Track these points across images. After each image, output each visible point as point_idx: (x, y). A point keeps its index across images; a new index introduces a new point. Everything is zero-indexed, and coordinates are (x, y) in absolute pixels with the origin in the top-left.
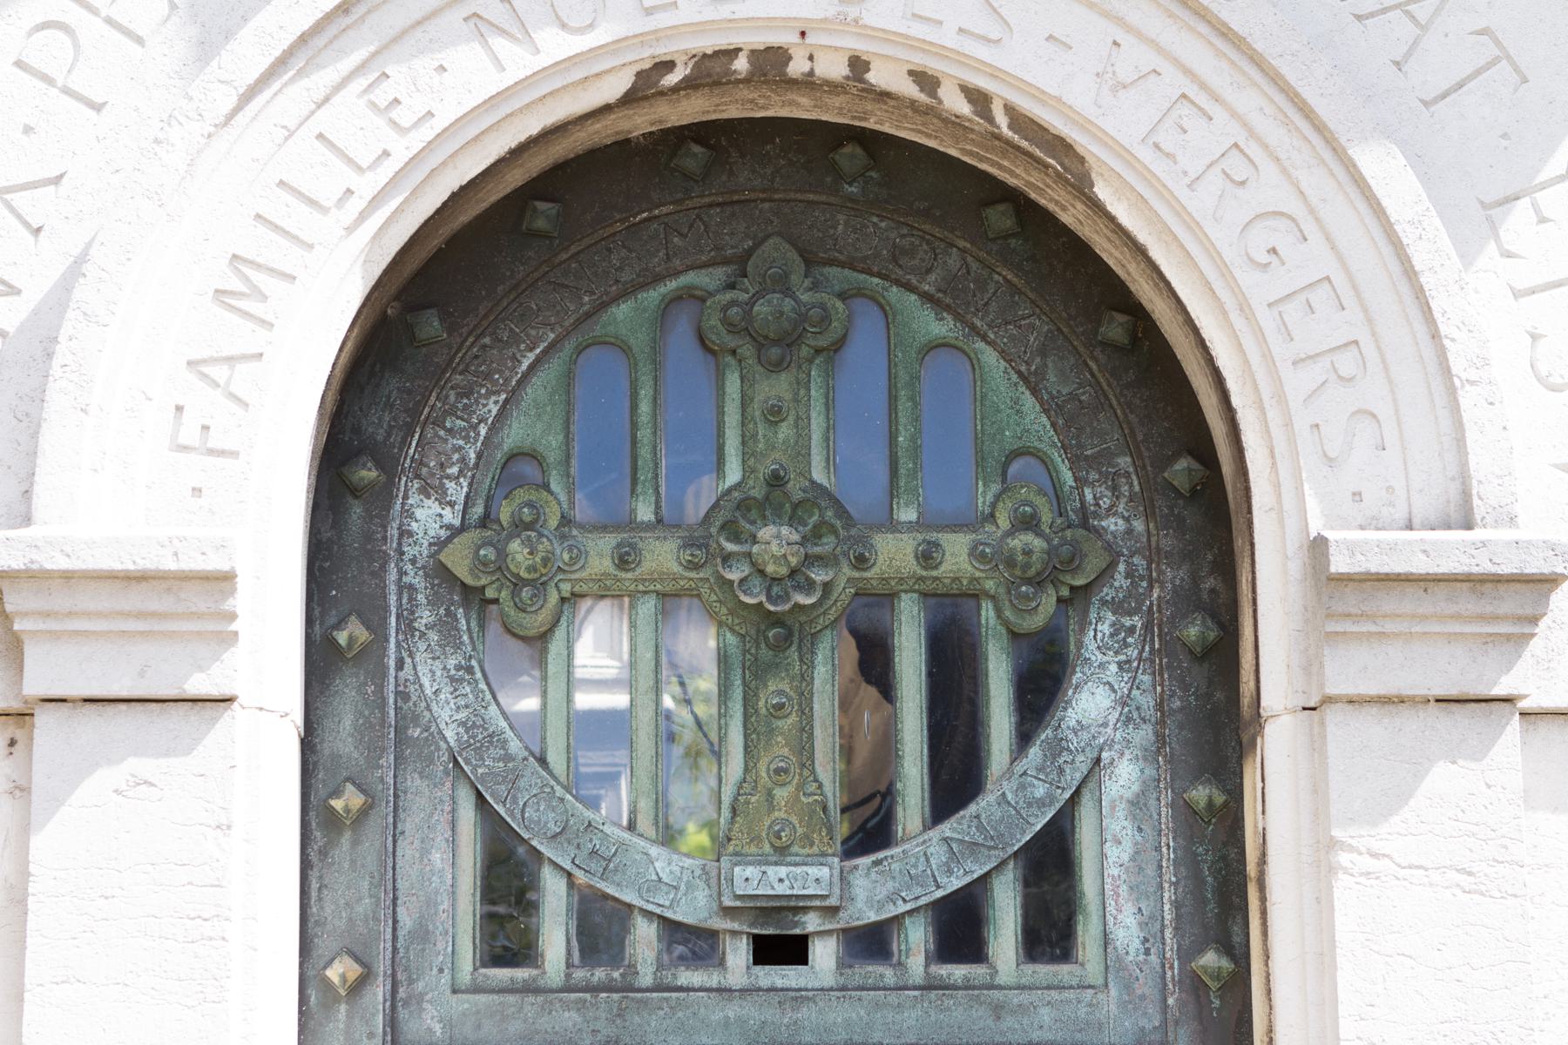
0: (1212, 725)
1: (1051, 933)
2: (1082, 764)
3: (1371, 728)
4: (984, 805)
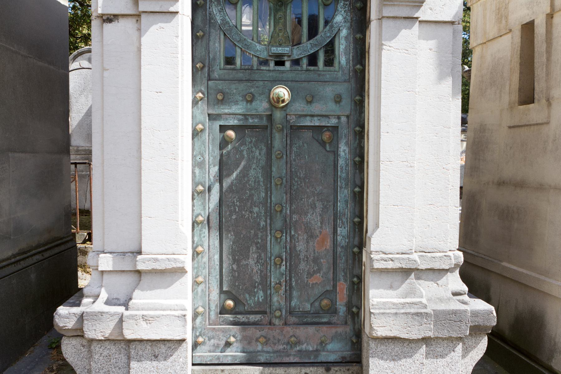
0: (361, 23)
1: (329, 62)
2: (337, 30)
3: (391, 23)
4: (318, 37)
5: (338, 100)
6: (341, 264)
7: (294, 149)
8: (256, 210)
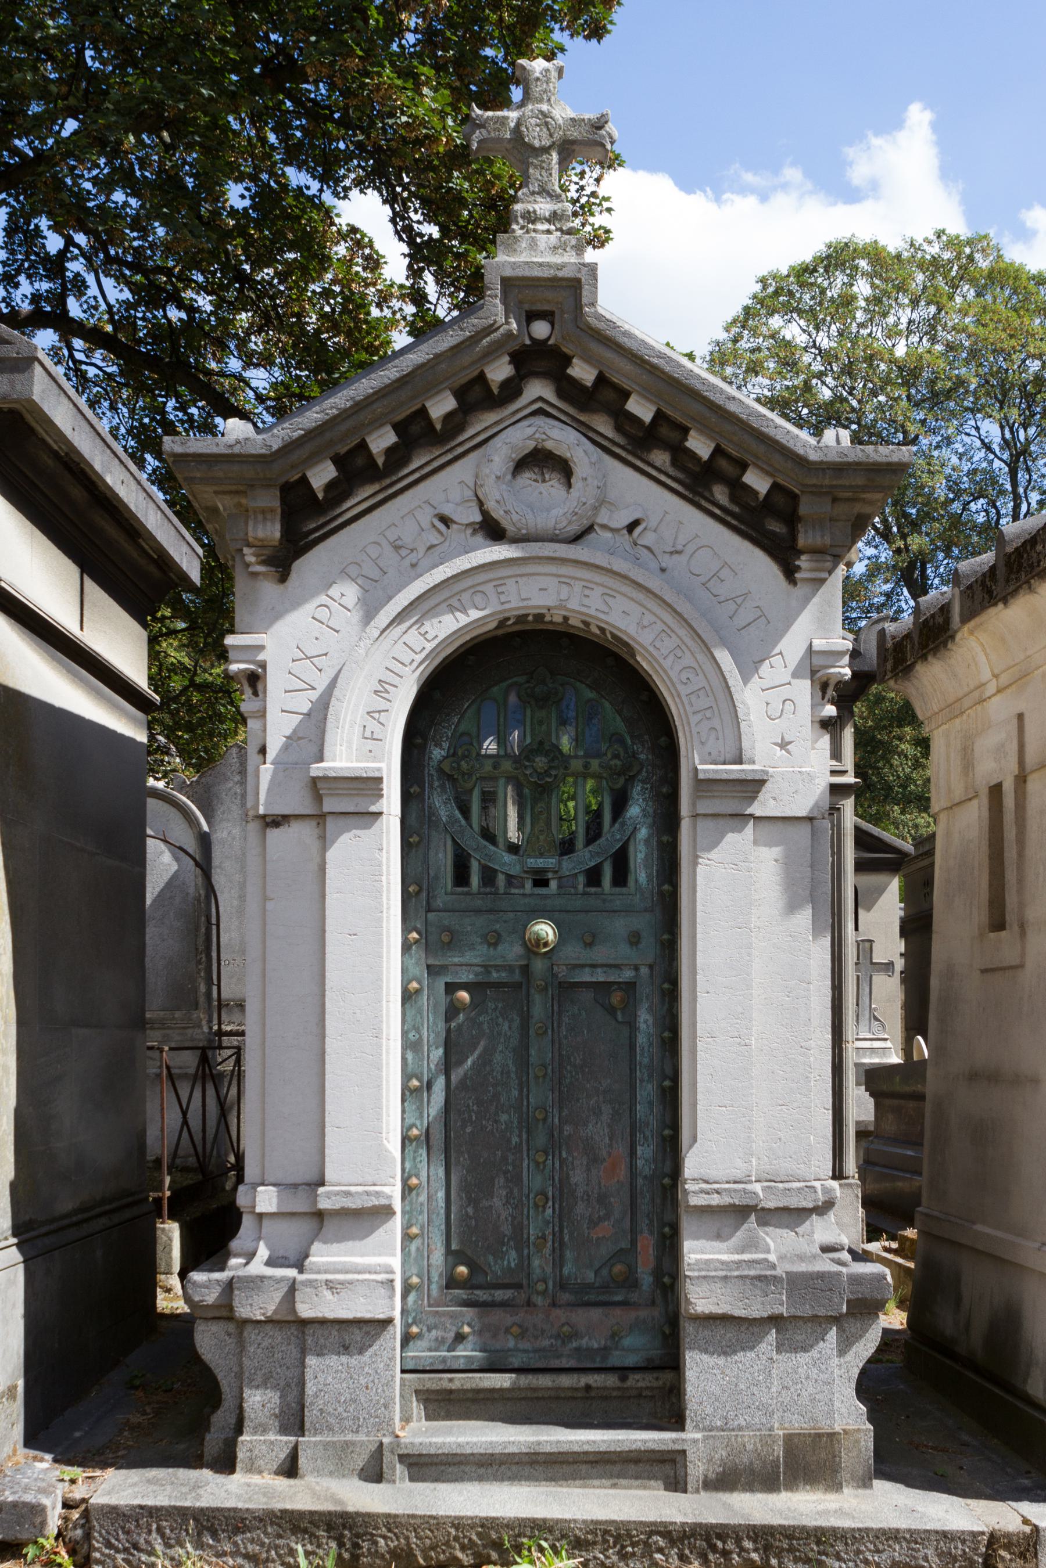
0: (668, 821)
1: (621, 877)
2: (631, 828)
3: (710, 823)
4: (601, 841)
5: (634, 939)
6: (644, 1205)
7: (566, 1020)
8: (504, 1117)
